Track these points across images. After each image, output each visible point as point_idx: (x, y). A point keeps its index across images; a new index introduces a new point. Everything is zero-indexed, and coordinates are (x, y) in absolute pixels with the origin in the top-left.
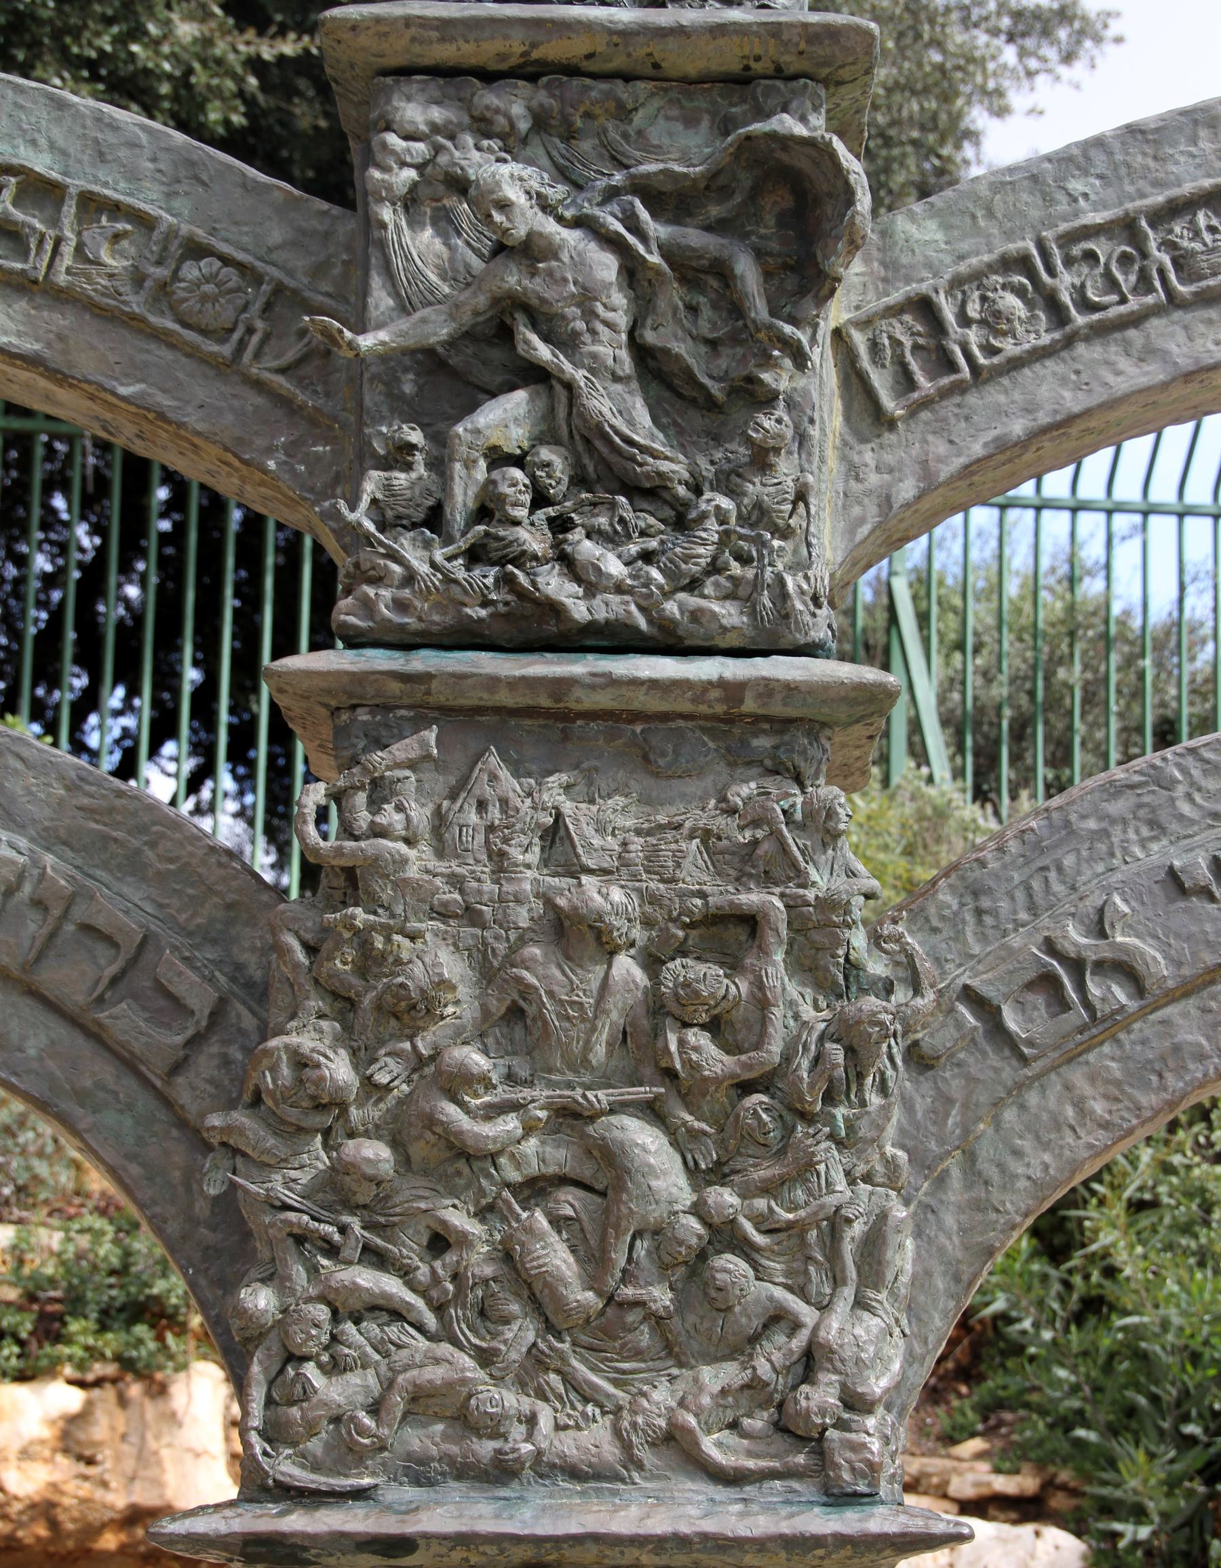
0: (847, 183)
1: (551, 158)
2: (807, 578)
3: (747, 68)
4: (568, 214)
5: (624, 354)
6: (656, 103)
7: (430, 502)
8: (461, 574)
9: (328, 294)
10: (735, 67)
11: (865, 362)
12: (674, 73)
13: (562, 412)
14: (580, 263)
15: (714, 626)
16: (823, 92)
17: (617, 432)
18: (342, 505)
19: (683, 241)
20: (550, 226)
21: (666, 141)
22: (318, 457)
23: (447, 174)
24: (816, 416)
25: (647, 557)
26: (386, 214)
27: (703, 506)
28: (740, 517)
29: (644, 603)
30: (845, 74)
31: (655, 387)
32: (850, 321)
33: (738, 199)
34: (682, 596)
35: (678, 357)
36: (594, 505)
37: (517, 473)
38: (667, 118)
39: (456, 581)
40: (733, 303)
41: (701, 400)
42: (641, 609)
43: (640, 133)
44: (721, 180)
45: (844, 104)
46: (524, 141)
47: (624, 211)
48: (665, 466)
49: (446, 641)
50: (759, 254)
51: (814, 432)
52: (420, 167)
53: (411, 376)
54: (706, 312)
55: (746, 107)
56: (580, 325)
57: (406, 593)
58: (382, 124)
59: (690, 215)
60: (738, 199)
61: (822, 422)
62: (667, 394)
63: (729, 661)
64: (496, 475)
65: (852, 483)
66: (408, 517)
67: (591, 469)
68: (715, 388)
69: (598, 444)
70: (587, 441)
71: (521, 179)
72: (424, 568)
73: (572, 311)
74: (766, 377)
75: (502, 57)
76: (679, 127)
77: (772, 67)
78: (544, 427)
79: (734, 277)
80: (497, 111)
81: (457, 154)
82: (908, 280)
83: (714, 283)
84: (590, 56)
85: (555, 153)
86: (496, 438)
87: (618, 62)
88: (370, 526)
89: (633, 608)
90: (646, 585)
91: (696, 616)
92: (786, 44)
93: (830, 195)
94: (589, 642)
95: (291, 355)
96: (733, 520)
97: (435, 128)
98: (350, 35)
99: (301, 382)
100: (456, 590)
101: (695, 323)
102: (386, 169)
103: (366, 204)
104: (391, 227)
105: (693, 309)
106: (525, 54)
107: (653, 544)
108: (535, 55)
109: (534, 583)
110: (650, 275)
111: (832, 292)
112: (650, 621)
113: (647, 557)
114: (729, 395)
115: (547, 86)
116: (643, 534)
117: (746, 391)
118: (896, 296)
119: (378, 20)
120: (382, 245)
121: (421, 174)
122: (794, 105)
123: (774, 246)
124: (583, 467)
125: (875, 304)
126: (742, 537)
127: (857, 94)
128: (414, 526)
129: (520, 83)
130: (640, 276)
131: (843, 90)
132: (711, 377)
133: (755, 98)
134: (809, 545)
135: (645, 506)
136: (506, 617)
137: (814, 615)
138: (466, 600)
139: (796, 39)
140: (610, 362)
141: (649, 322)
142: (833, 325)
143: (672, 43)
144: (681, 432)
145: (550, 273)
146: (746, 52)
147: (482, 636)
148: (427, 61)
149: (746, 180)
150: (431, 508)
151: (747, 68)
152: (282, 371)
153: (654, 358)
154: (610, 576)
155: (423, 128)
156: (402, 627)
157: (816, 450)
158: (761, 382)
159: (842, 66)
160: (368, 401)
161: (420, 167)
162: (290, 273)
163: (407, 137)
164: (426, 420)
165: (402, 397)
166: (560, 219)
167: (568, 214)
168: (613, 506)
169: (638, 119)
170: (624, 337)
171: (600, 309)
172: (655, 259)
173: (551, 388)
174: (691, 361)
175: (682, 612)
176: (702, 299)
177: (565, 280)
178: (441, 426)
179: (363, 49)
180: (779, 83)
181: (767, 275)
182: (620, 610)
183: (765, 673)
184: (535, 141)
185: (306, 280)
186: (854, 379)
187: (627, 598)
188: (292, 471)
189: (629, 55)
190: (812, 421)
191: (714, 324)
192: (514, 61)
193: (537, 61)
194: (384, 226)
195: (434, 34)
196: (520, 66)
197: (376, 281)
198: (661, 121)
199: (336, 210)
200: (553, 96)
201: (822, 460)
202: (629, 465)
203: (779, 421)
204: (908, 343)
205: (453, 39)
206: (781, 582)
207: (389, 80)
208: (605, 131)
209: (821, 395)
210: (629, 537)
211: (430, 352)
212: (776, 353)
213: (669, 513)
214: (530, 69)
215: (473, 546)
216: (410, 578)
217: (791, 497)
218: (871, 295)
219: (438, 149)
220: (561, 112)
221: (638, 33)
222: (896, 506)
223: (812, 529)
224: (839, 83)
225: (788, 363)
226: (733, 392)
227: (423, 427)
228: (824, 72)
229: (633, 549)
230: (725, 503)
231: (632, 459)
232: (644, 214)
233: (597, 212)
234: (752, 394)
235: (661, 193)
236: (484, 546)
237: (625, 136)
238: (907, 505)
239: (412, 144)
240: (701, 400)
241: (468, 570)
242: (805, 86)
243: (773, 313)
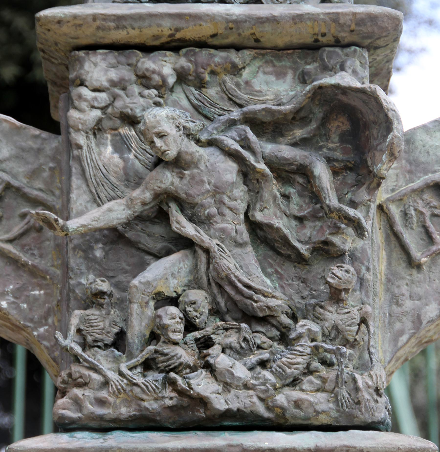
0: (386, 115)
1: (189, 100)
2: (370, 376)
3: (317, 41)
4: (204, 137)
5: (243, 228)
6: (257, 63)
7: (116, 330)
8: (140, 380)
9: (41, 190)
10: (309, 40)
11: (399, 227)
12: (269, 45)
13: (203, 267)
14: (211, 171)
15: (311, 410)
16: (366, 54)
17: (240, 281)
18: (59, 335)
19: (279, 154)
20: (193, 147)
21: (264, 88)
22: (36, 299)
23: (121, 113)
24: (371, 267)
25: (263, 364)
26: (81, 139)
27: (300, 330)
28: (324, 335)
29: (262, 396)
30: (380, 42)
31: (263, 249)
32: (388, 200)
33: (314, 125)
34: (287, 391)
35: (278, 230)
36: (226, 329)
37: (173, 310)
38: (265, 73)
39: (136, 385)
40: (313, 192)
41: (293, 256)
42: (262, 400)
43: (247, 83)
44: (302, 114)
45: (378, 59)
46: (172, 90)
47: (240, 135)
48: (272, 302)
49: (131, 425)
50: (329, 160)
51: (369, 276)
52: (103, 109)
53: (100, 245)
54: (295, 199)
55: (316, 65)
56: (213, 210)
57: (103, 394)
58: (78, 82)
59: (282, 135)
60: (314, 125)
61: (375, 269)
62: (270, 253)
63: (320, 434)
64: (160, 311)
65: (394, 307)
66: (102, 340)
67: (223, 304)
68: (303, 249)
69: (228, 289)
70: (220, 287)
71: (174, 119)
72: (113, 376)
73: (208, 201)
74: (336, 240)
75: (156, 37)
76: (273, 78)
77: (333, 40)
78: (191, 278)
79: (314, 177)
80: (154, 72)
81: (128, 100)
82: (426, 172)
83: (301, 180)
84: (214, 36)
85: (191, 97)
86: (161, 288)
87: (232, 39)
88: (78, 349)
89: (255, 399)
90: (264, 384)
91: (297, 404)
92: (342, 26)
93: (375, 123)
94: (226, 423)
95: (17, 230)
96: (320, 338)
97: (114, 84)
98: (57, 26)
99: (23, 247)
100: (137, 390)
101: (288, 206)
102: (80, 110)
103: (69, 133)
104: (85, 148)
105: (286, 197)
106: (171, 36)
107: (266, 355)
108: (178, 36)
109: (189, 385)
110: (258, 176)
111: (379, 185)
112: (269, 408)
113: (263, 364)
114: (312, 253)
115: (186, 55)
116: (259, 347)
117: (323, 250)
118: (418, 183)
119: (75, 17)
120: (79, 160)
121: (104, 113)
122: (348, 63)
123: (338, 155)
124: (218, 303)
125: (405, 188)
126: (326, 350)
127: (389, 51)
128: (107, 346)
129: (168, 53)
130: (251, 177)
131: (379, 51)
132: (300, 241)
133: (322, 60)
134: (370, 353)
135: (260, 328)
136: (171, 408)
137: (377, 401)
138: (144, 397)
139: (349, 23)
140: (234, 234)
141: (258, 206)
142: (378, 202)
143: (268, 28)
144: (281, 277)
145: (193, 177)
146: (317, 30)
147: (155, 421)
148: (107, 41)
149: (319, 113)
150: (117, 334)
151: (317, 41)
152: (10, 241)
153: (262, 229)
154: (239, 378)
155: (106, 84)
156: (101, 418)
157: (371, 289)
158: (333, 245)
159: (379, 38)
160: (72, 263)
161: (103, 109)
162: (15, 176)
163: (95, 90)
164: (111, 274)
165: (94, 260)
166: (198, 142)
167: (204, 137)
168: (239, 330)
169: (246, 74)
170: (242, 217)
171: (226, 200)
172: (262, 166)
173: (195, 252)
174: (286, 231)
175: (289, 402)
176: (292, 190)
177: (202, 182)
178: (122, 278)
179: (65, 34)
180: (338, 50)
181: (335, 173)
182: (247, 401)
183: (346, 443)
184: (178, 89)
185: (25, 181)
186: (393, 238)
187: (251, 392)
188: (18, 307)
189: (239, 35)
190: (368, 269)
191: (301, 206)
192: (164, 40)
193: (179, 40)
194: (80, 147)
195: (112, 24)
196: (168, 43)
197: (76, 182)
198: (261, 75)
199: (45, 134)
200: (190, 61)
201: (375, 295)
202: (249, 302)
203: (347, 271)
204: (427, 213)
205: (124, 27)
206: (354, 380)
207: (82, 53)
208: (224, 82)
209: (373, 251)
210: (251, 350)
211: (113, 230)
212: (343, 226)
213: (275, 333)
214: (174, 44)
215: (147, 359)
216: (106, 383)
217: (357, 321)
218: (402, 182)
219: (115, 97)
220: (196, 71)
221: (246, 21)
222: (424, 322)
223: (372, 343)
224: (376, 48)
225: (350, 231)
226: (314, 250)
227: (109, 278)
228: (367, 42)
229: (253, 359)
230: (315, 327)
231: (251, 298)
232: (251, 135)
233: (221, 137)
234: (327, 252)
235: (263, 123)
236: (154, 359)
237: (238, 85)
238: (432, 321)
239: (97, 94)
240: (293, 256)
241: (145, 376)
242: (355, 51)
243: (340, 200)
